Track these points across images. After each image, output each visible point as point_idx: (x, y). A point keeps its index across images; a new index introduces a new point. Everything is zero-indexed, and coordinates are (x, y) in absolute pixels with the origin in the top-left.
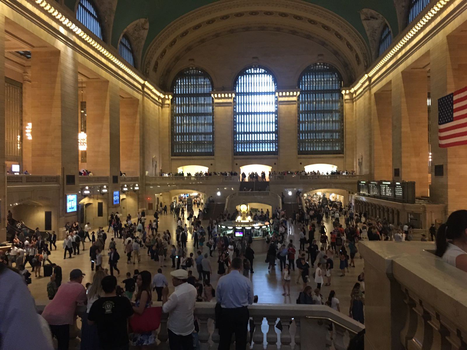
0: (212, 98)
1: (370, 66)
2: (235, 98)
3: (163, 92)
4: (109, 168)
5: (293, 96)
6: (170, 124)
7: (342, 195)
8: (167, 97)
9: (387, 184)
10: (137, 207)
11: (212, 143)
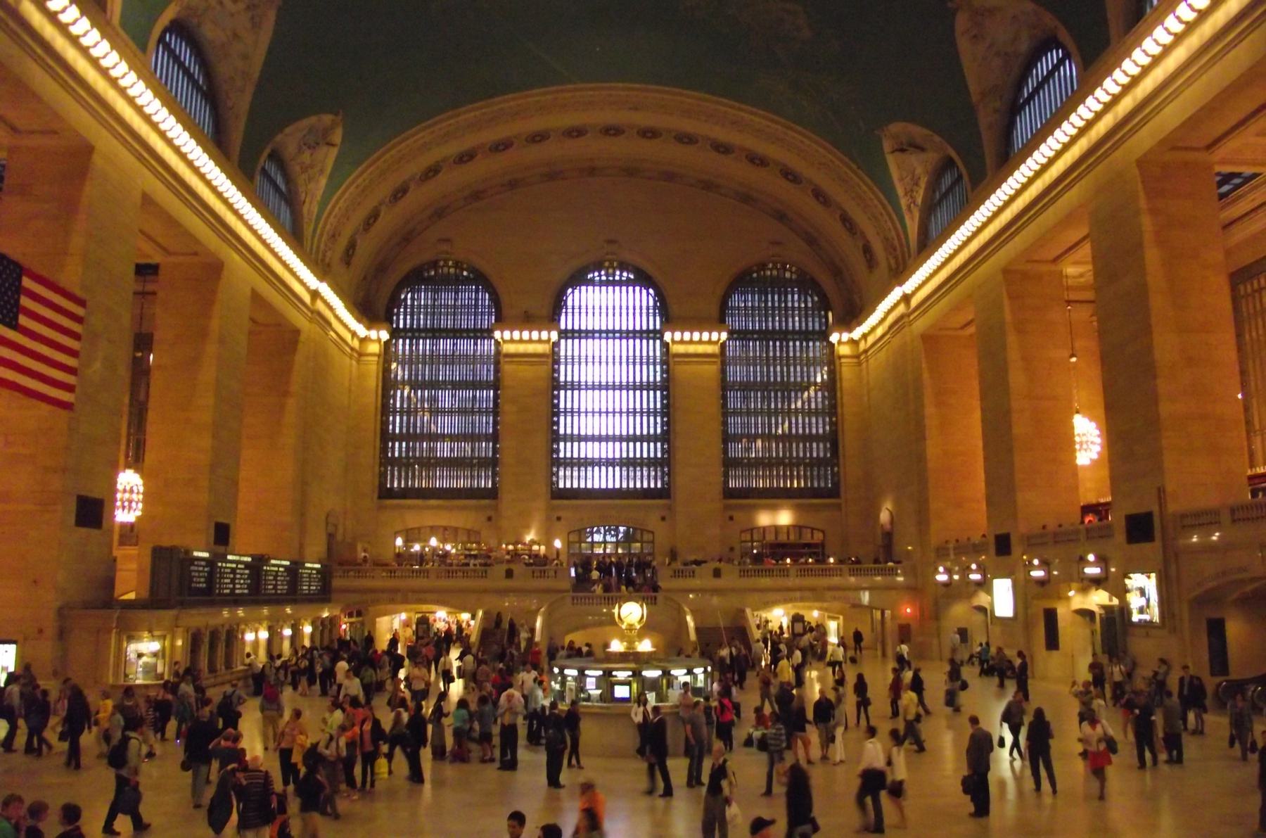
0: (496, 341)
1: (905, 268)
2: (556, 344)
5: (710, 342)
8: (373, 334)
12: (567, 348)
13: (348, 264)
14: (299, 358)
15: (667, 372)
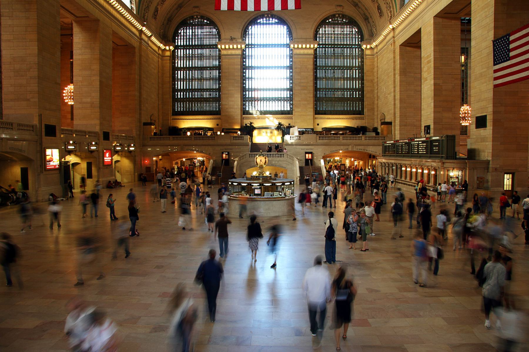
3: (163, 42)
4: (98, 122)
6: (171, 79)
7: (361, 160)
8: (167, 48)
9: (420, 141)
10: (133, 170)
11: (218, 100)
12: (248, 52)
13: (155, 18)
14: (137, 59)
15: (292, 61)
